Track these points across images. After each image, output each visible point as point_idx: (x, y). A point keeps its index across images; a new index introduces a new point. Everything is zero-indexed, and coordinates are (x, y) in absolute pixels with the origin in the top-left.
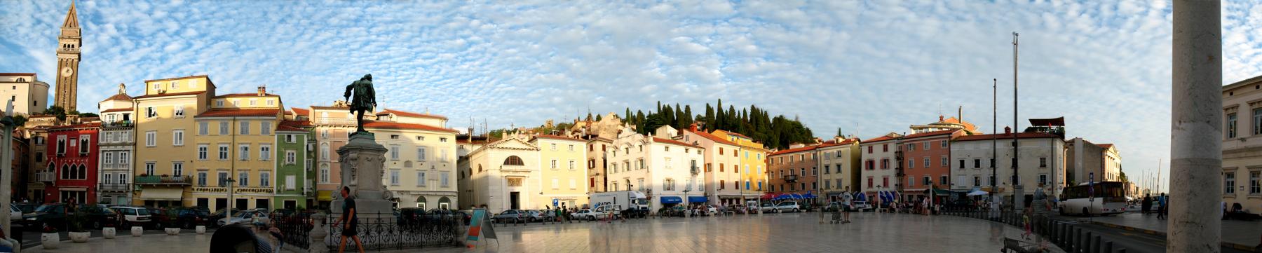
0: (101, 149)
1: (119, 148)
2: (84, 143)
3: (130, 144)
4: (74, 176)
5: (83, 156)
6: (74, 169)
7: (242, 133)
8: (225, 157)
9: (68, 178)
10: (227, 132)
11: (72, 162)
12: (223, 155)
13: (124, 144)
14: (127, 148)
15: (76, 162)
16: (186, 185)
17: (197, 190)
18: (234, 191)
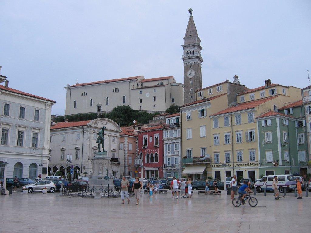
0: (165, 142)
1: (174, 141)
2: (157, 139)
3: (178, 138)
4: (152, 161)
5: (156, 147)
6: (152, 155)
7: (237, 123)
8: (229, 142)
9: (149, 162)
10: (228, 125)
11: (151, 152)
12: (227, 141)
13: (175, 139)
14: (177, 141)
15: (153, 151)
16: (206, 162)
17: (215, 166)
18: (235, 166)
